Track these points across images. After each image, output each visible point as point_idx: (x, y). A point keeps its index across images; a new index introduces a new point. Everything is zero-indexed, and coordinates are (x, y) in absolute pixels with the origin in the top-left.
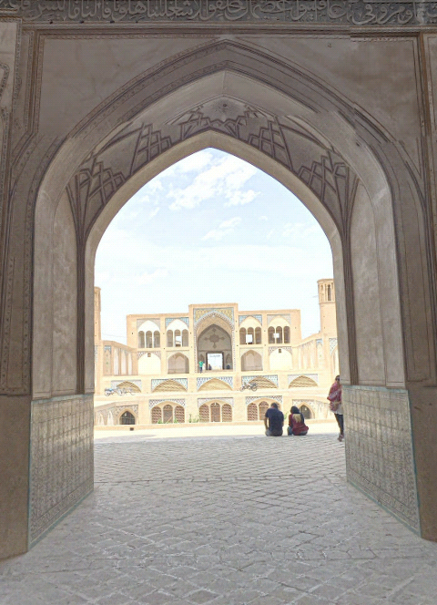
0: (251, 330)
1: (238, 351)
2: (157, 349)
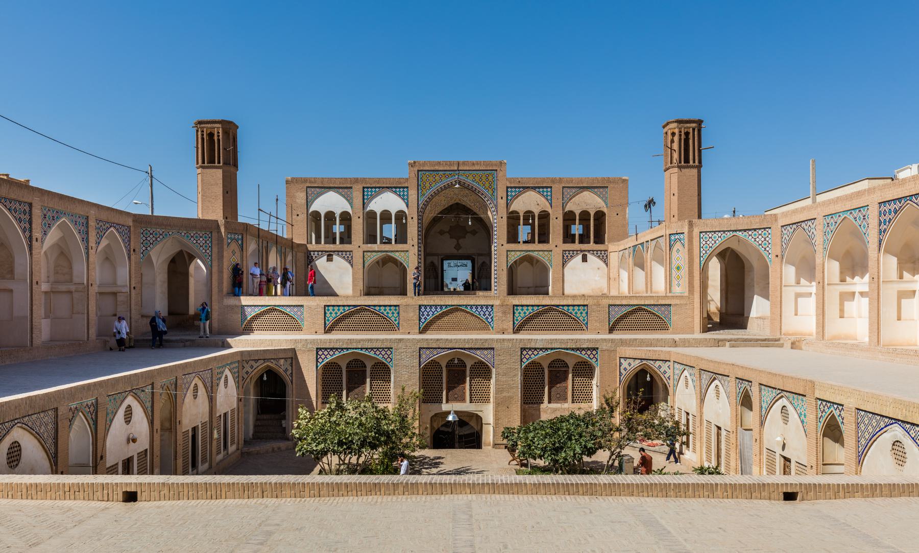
0: (529, 214)
1: (502, 254)
2: (346, 247)
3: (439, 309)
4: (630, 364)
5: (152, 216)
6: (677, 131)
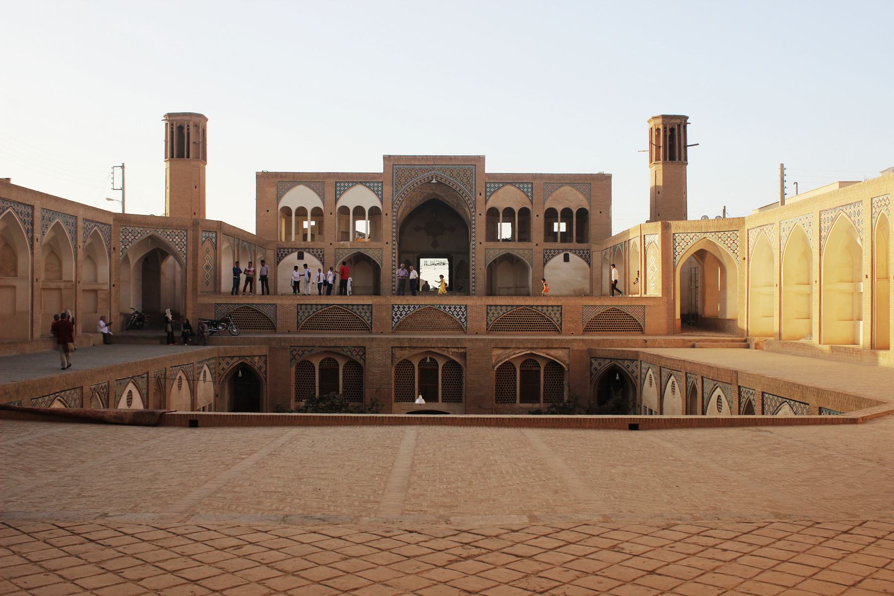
0: (509, 214)
3: (412, 309)
4: (600, 364)
5: (123, 214)
6: (661, 127)
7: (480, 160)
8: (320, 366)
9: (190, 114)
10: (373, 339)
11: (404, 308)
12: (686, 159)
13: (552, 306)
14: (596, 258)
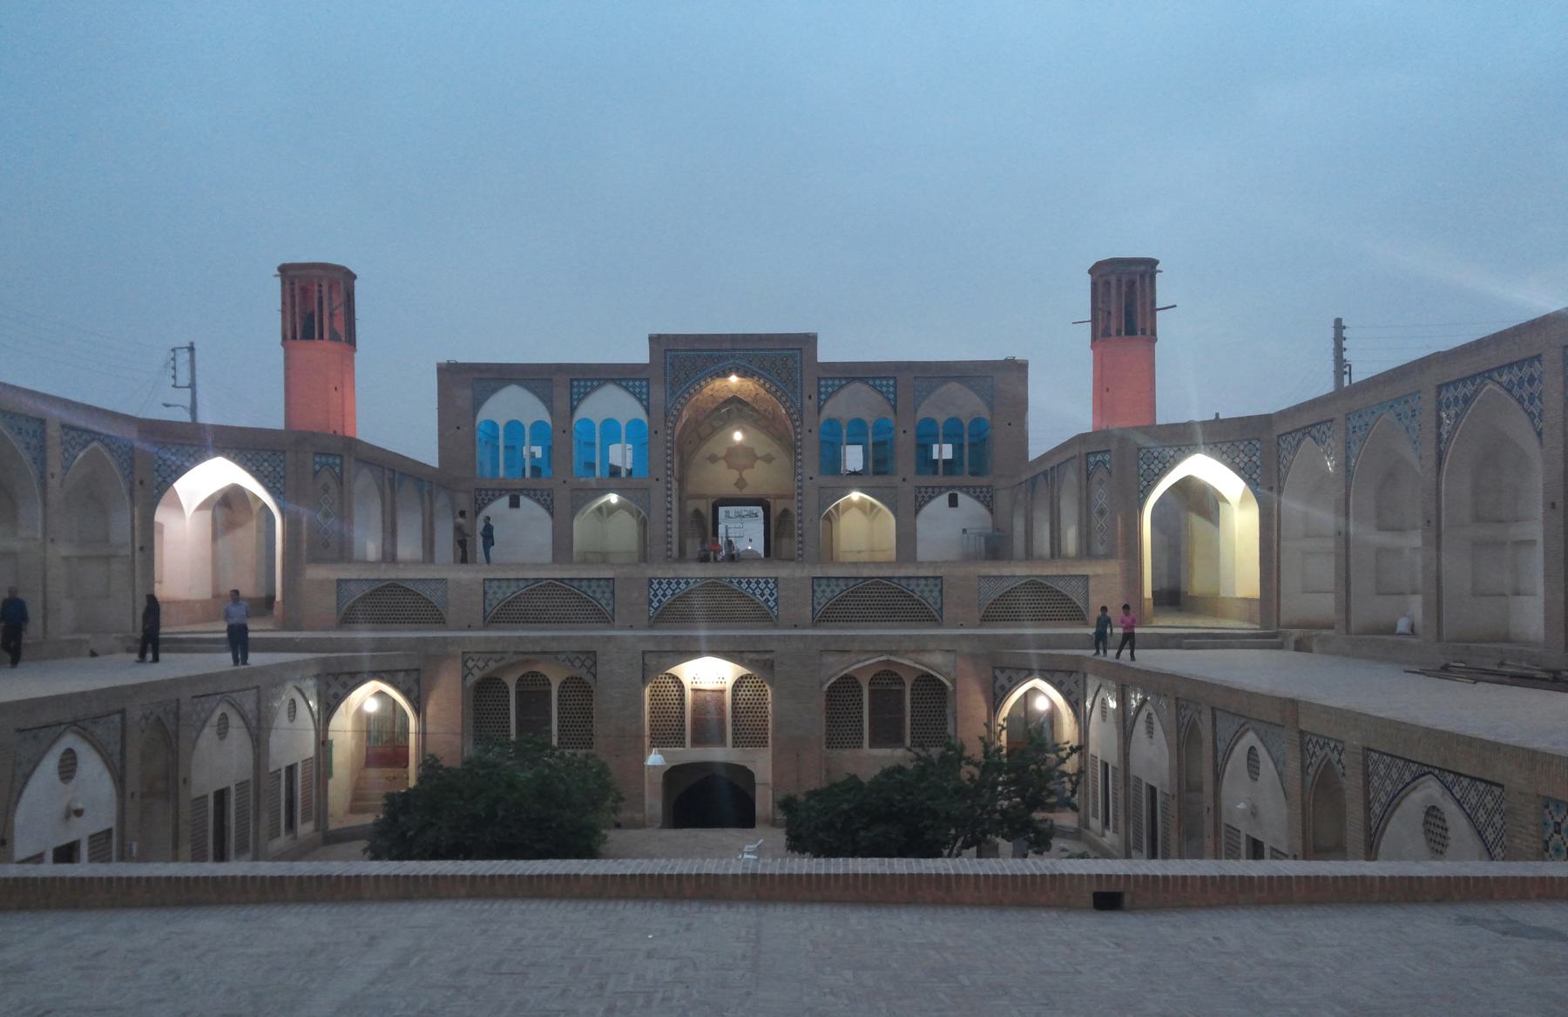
3: (683, 586)
7: (810, 340)
8: (518, 686)
9: (324, 267)
10: (609, 638)
11: (669, 583)
12: (1154, 333)
13: (926, 578)
14: (1003, 499)
